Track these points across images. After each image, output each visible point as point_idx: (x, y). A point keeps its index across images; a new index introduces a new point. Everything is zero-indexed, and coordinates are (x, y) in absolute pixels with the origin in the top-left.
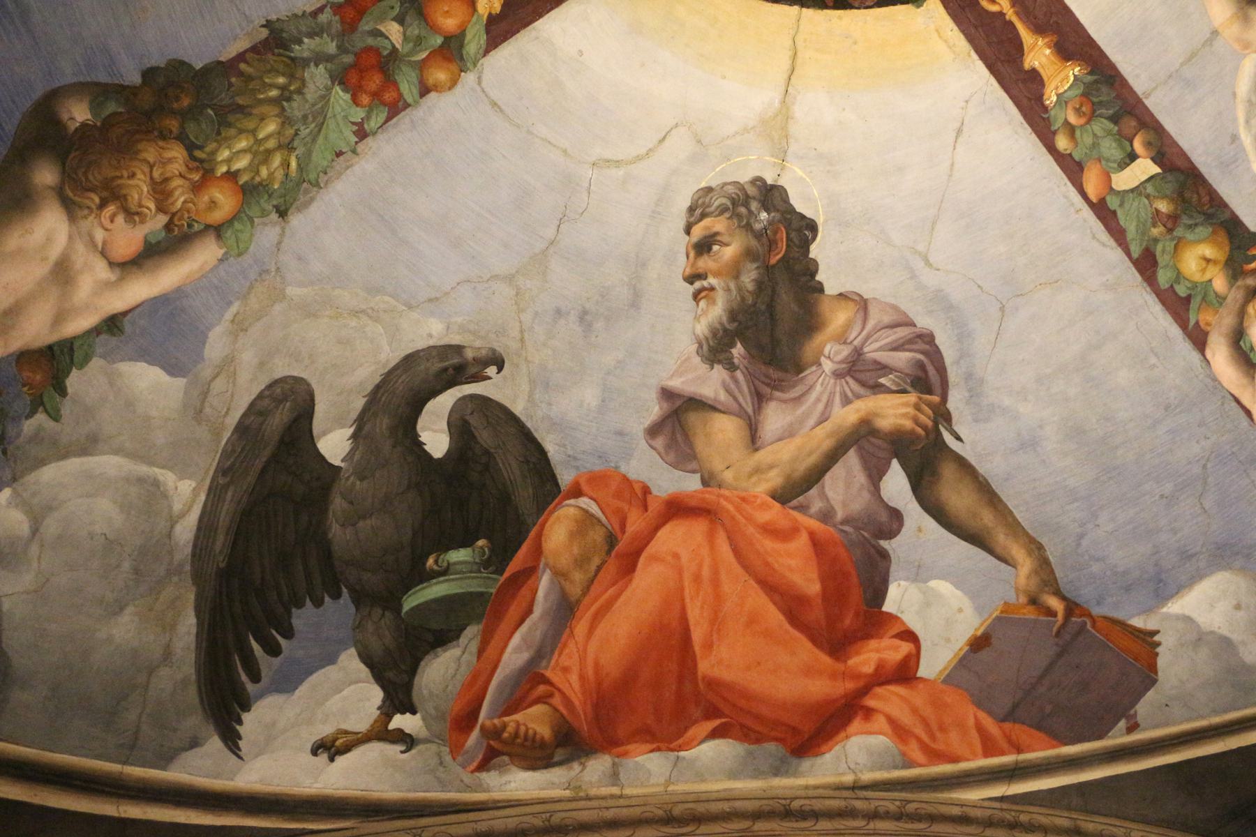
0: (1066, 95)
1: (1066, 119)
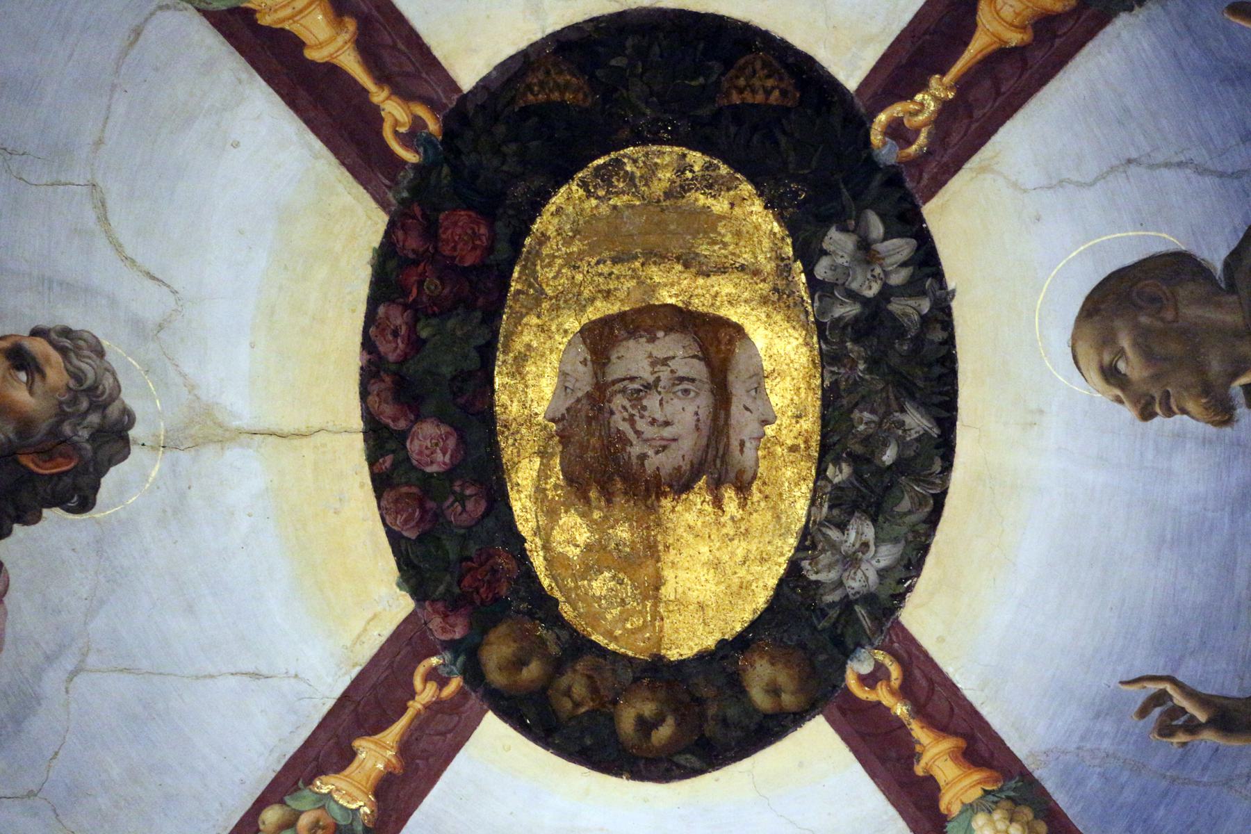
0: (332, 803)
1: (301, 813)
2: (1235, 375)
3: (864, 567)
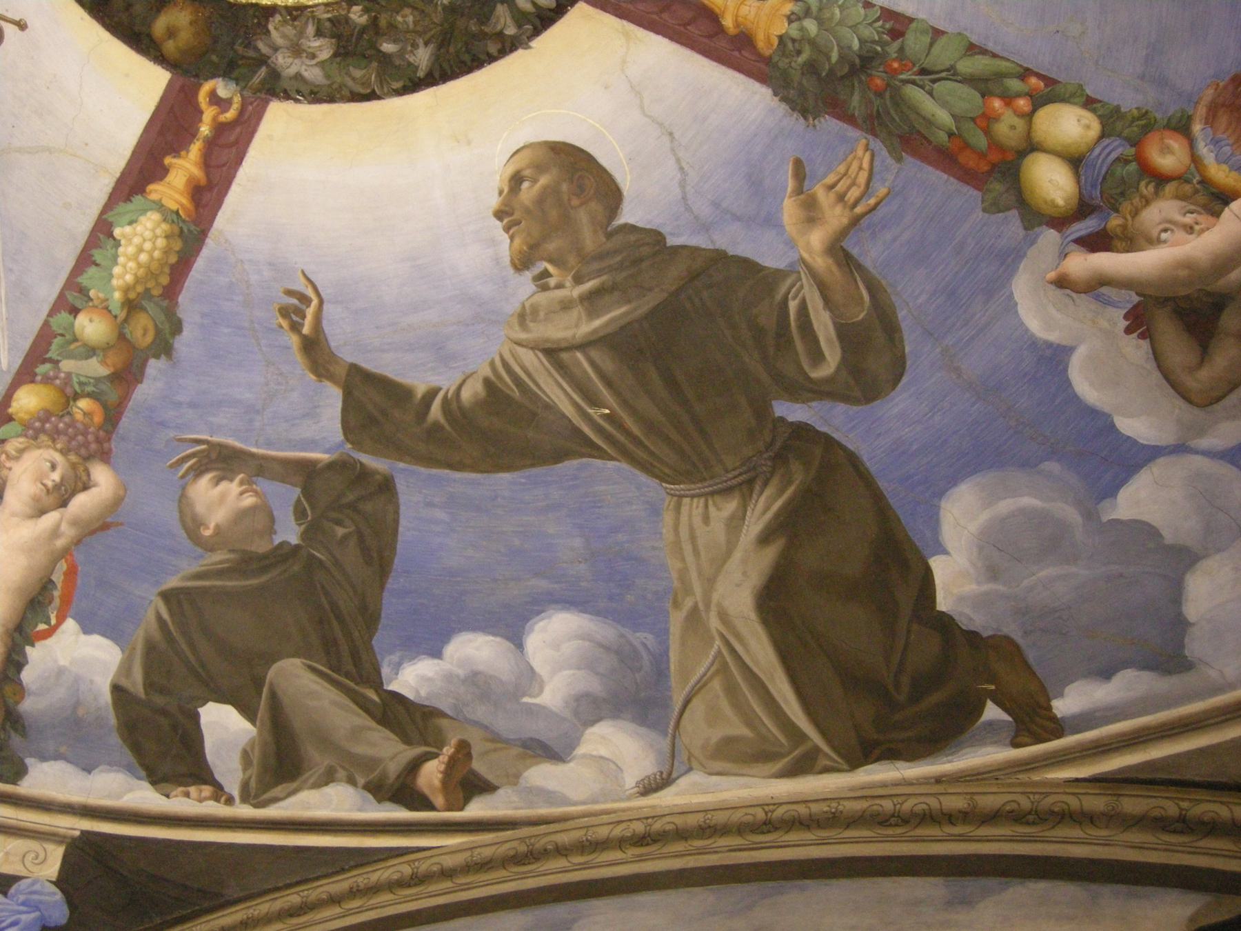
2: (551, 261)
3: (296, 61)
